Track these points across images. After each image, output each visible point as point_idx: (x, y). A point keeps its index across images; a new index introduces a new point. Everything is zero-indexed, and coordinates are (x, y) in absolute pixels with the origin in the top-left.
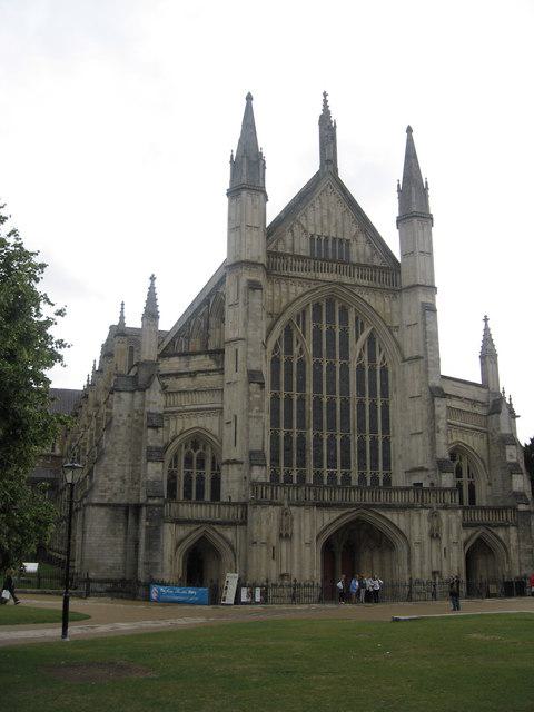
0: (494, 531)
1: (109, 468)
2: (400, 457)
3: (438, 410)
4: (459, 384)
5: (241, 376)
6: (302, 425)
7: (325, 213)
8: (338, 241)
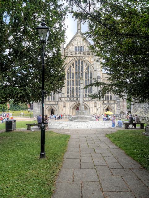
7: (78, 41)
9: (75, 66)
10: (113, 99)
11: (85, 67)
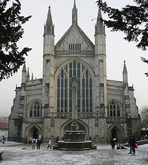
1: (14, 110)
4: (115, 82)
6: (66, 96)
7: (73, 37)
8: (77, 44)
9: (69, 69)
10: (121, 116)
11: (83, 71)
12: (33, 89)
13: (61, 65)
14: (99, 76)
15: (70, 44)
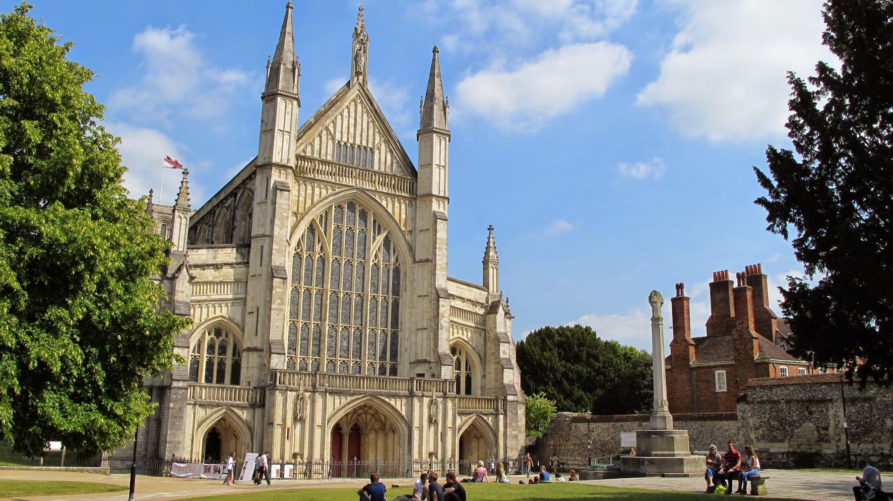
0: (485, 418)
2: (406, 348)
3: (441, 310)
5: (264, 270)
7: (352, 121)
11: (374, 239)
12: (210, 279)
13: (313, 205)
14: (430, 263)
15: (343, 144)
